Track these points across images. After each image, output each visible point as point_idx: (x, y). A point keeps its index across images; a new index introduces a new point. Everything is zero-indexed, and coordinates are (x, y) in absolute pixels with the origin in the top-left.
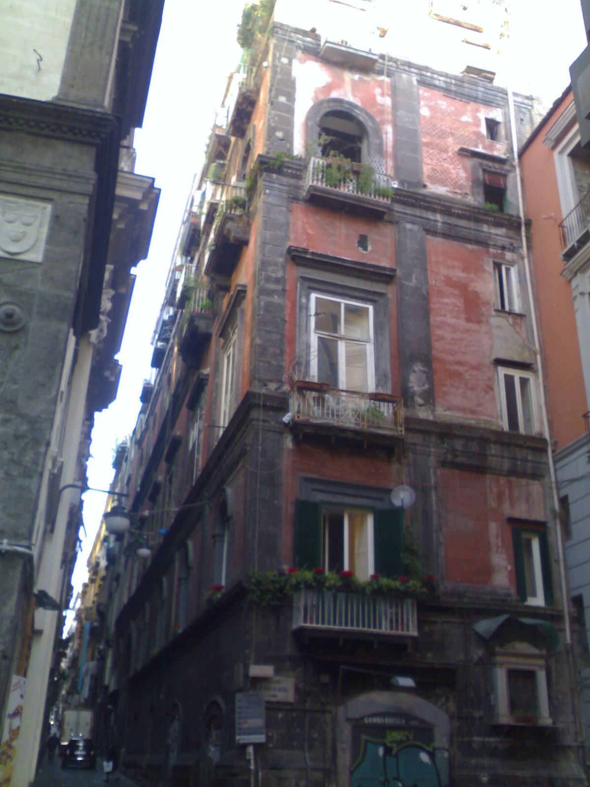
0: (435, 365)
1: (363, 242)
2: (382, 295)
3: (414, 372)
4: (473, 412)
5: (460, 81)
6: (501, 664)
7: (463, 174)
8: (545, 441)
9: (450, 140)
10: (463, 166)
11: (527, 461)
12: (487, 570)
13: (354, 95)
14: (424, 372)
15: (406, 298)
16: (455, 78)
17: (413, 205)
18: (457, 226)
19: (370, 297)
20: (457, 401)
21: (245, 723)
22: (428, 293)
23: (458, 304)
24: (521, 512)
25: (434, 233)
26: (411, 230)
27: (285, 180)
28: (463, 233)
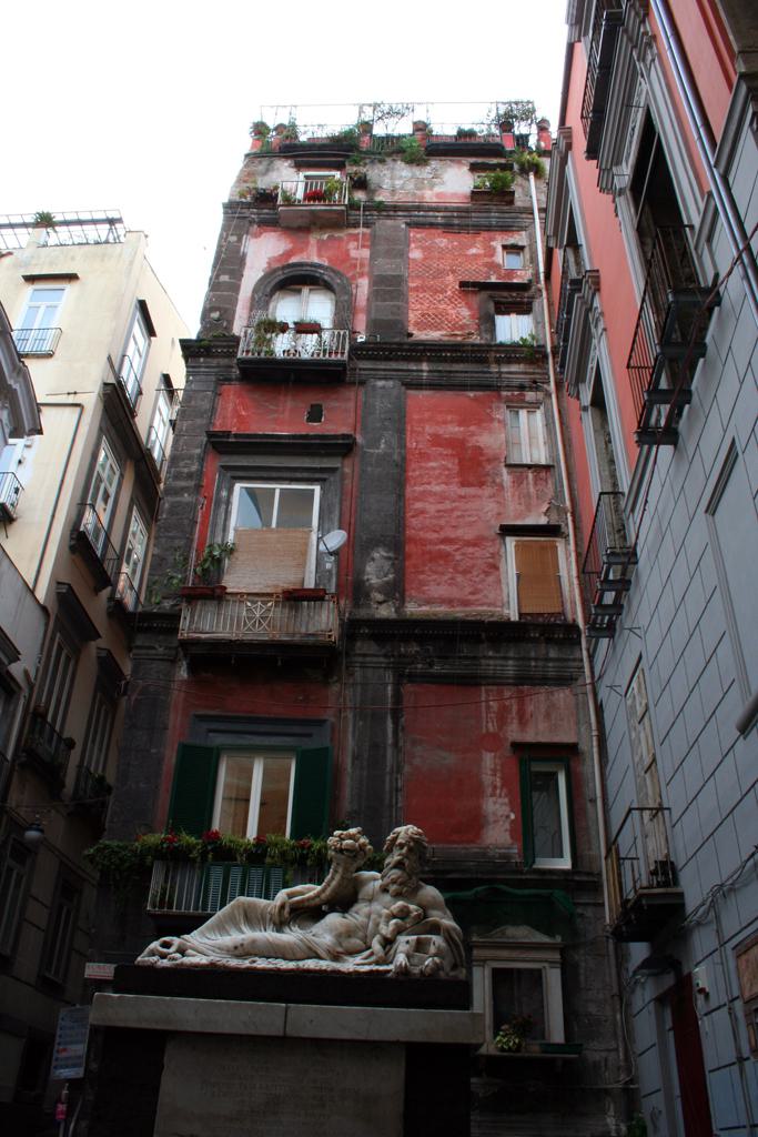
0: (409, 548)
1: (315, 414)
2: (333, 470)
3: (373, 559)
4: (465, 603)
5: (462, 212)
6: (484, 961)
7: (466, 312)
8: (574, 627)
9: (451, 278)
10: (466, 304)
11: (548, 660)
12: (476, 823)
13: (320, 256)
14: (389, 558)
15: (369, 469)
16: (458, 210)
17: (387, 359)
18: (450, 372)
19: (317, 476)
20: (436, 591)
21: (65, 1050)
22: (404, 459)
23: (450, 466)
24: (538, 733)
25: (419, 386)
26: (383, 387)
27: (215, 362)
28: (460, 378)
